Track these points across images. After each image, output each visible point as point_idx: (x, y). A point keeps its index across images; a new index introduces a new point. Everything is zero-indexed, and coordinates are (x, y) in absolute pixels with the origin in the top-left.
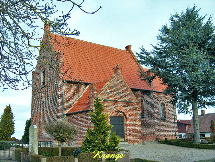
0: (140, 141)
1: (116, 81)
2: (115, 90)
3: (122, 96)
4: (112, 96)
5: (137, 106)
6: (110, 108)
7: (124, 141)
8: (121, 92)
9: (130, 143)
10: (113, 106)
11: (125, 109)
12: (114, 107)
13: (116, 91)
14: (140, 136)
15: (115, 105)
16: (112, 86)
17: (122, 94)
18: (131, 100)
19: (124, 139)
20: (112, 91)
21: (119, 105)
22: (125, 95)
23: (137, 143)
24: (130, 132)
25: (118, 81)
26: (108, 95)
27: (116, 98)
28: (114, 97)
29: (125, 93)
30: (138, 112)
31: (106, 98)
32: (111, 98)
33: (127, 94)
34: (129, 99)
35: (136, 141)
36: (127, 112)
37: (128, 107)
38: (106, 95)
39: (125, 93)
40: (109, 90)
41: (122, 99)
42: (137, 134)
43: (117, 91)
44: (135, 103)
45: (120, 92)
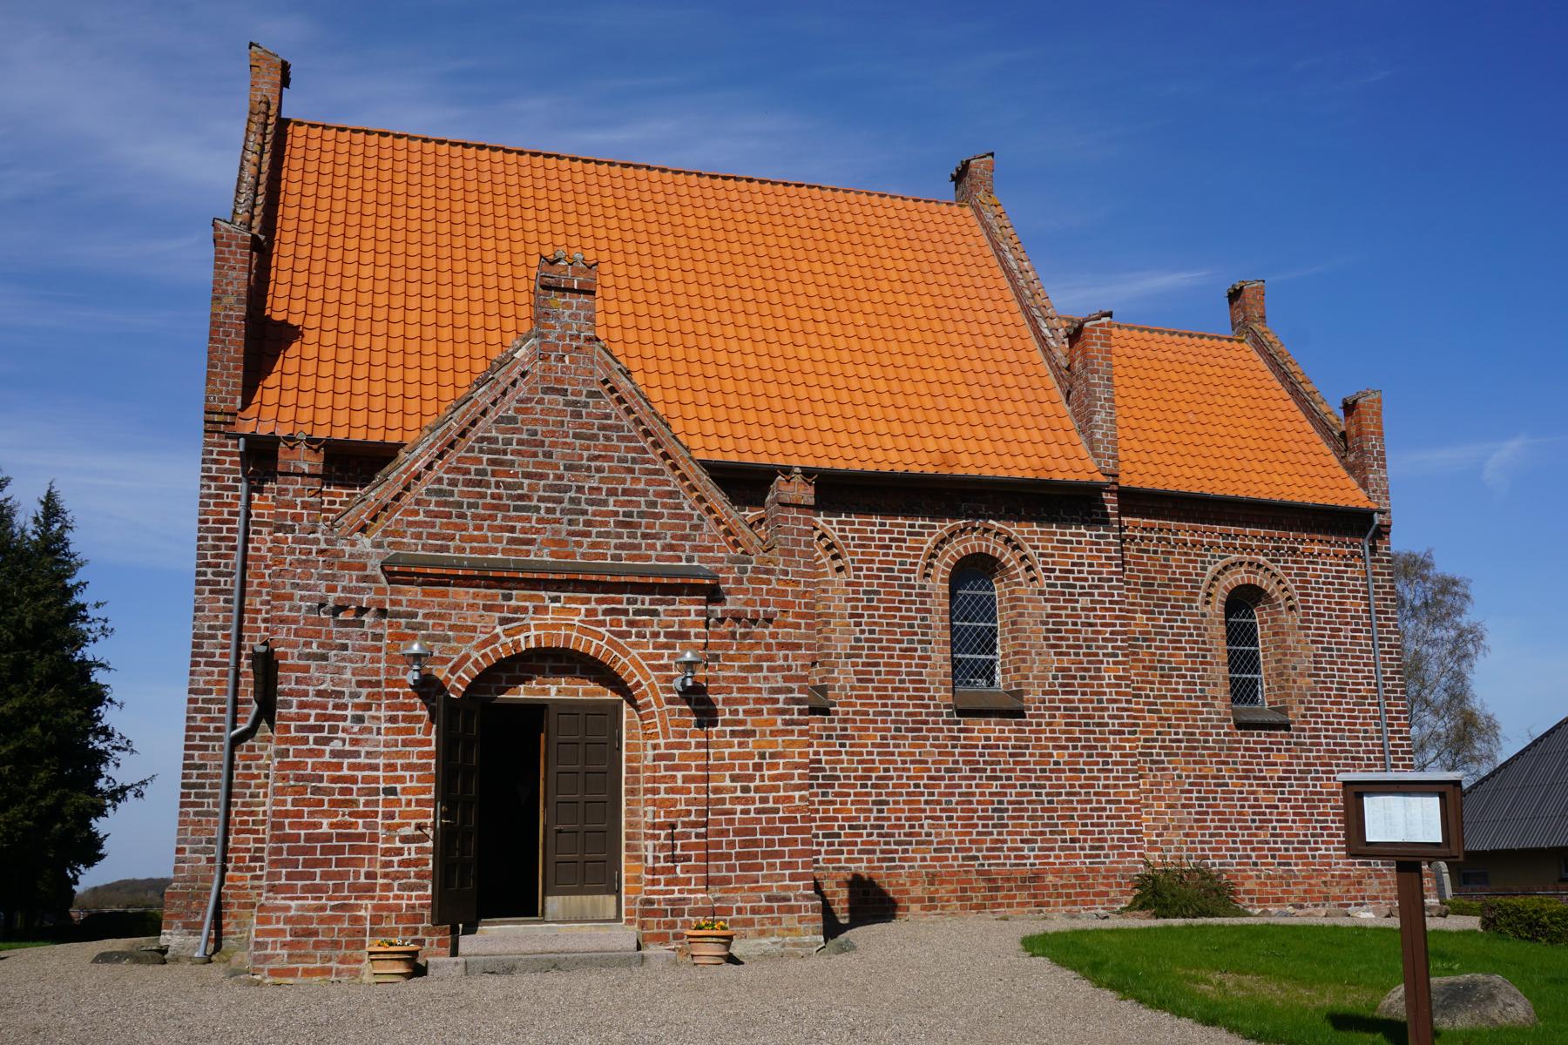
0: (788, 920)
1: (533, 390)
2: (515, 475)
3: (588, 523)
4: (480, 528)
5: (764, 603)
6: (452, 628)
7: (612, 914)
8: (580, 489)
9: (677, 937)
10: (487, 608)
11: (621, 635)
12: (503, 621)
13: (527, 475)
14: (793, 877)
15: (508, 598)
16: (482, 440)
17: (591, 502)
18: (695, 549)
19: (614, 898)
20: (479, 484)
21: (555, 600)
22: (628, 514)
23: (762, 933)
24: (672, 837)
25: (546, 391)
26: (436, 515)
27: (531, 542)
28: (502, 529)
29: (625, 492)
30: (771, 658)
31: (415, 546)
32: (472, 539)
33: (653, 504)
34: (671, 547)
35: (750, 923)
36: (644, 657)
37: (655, 613)
38: (421, 517)
39: (625, 492)
40: (458, 470)
41: (594, 545)
42: (766, 855)
43: (542, 477)
44: (739, 581)
45: (567, 489)
